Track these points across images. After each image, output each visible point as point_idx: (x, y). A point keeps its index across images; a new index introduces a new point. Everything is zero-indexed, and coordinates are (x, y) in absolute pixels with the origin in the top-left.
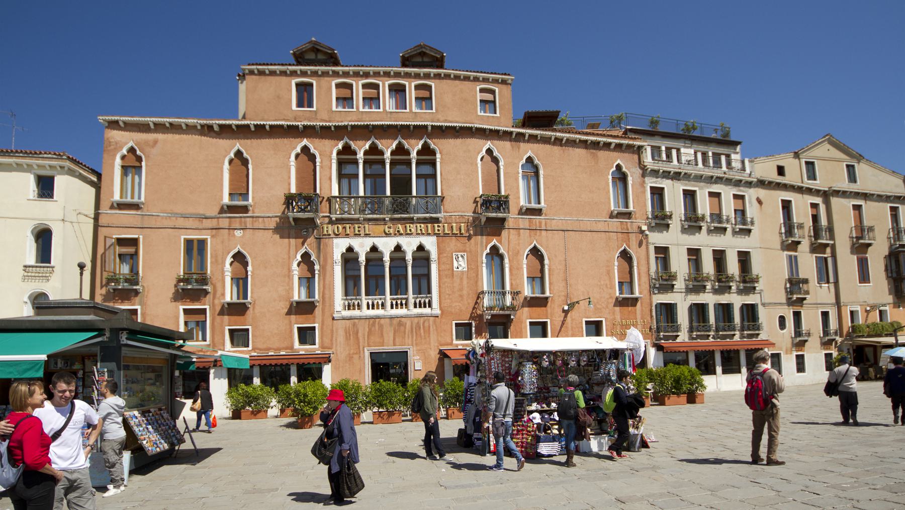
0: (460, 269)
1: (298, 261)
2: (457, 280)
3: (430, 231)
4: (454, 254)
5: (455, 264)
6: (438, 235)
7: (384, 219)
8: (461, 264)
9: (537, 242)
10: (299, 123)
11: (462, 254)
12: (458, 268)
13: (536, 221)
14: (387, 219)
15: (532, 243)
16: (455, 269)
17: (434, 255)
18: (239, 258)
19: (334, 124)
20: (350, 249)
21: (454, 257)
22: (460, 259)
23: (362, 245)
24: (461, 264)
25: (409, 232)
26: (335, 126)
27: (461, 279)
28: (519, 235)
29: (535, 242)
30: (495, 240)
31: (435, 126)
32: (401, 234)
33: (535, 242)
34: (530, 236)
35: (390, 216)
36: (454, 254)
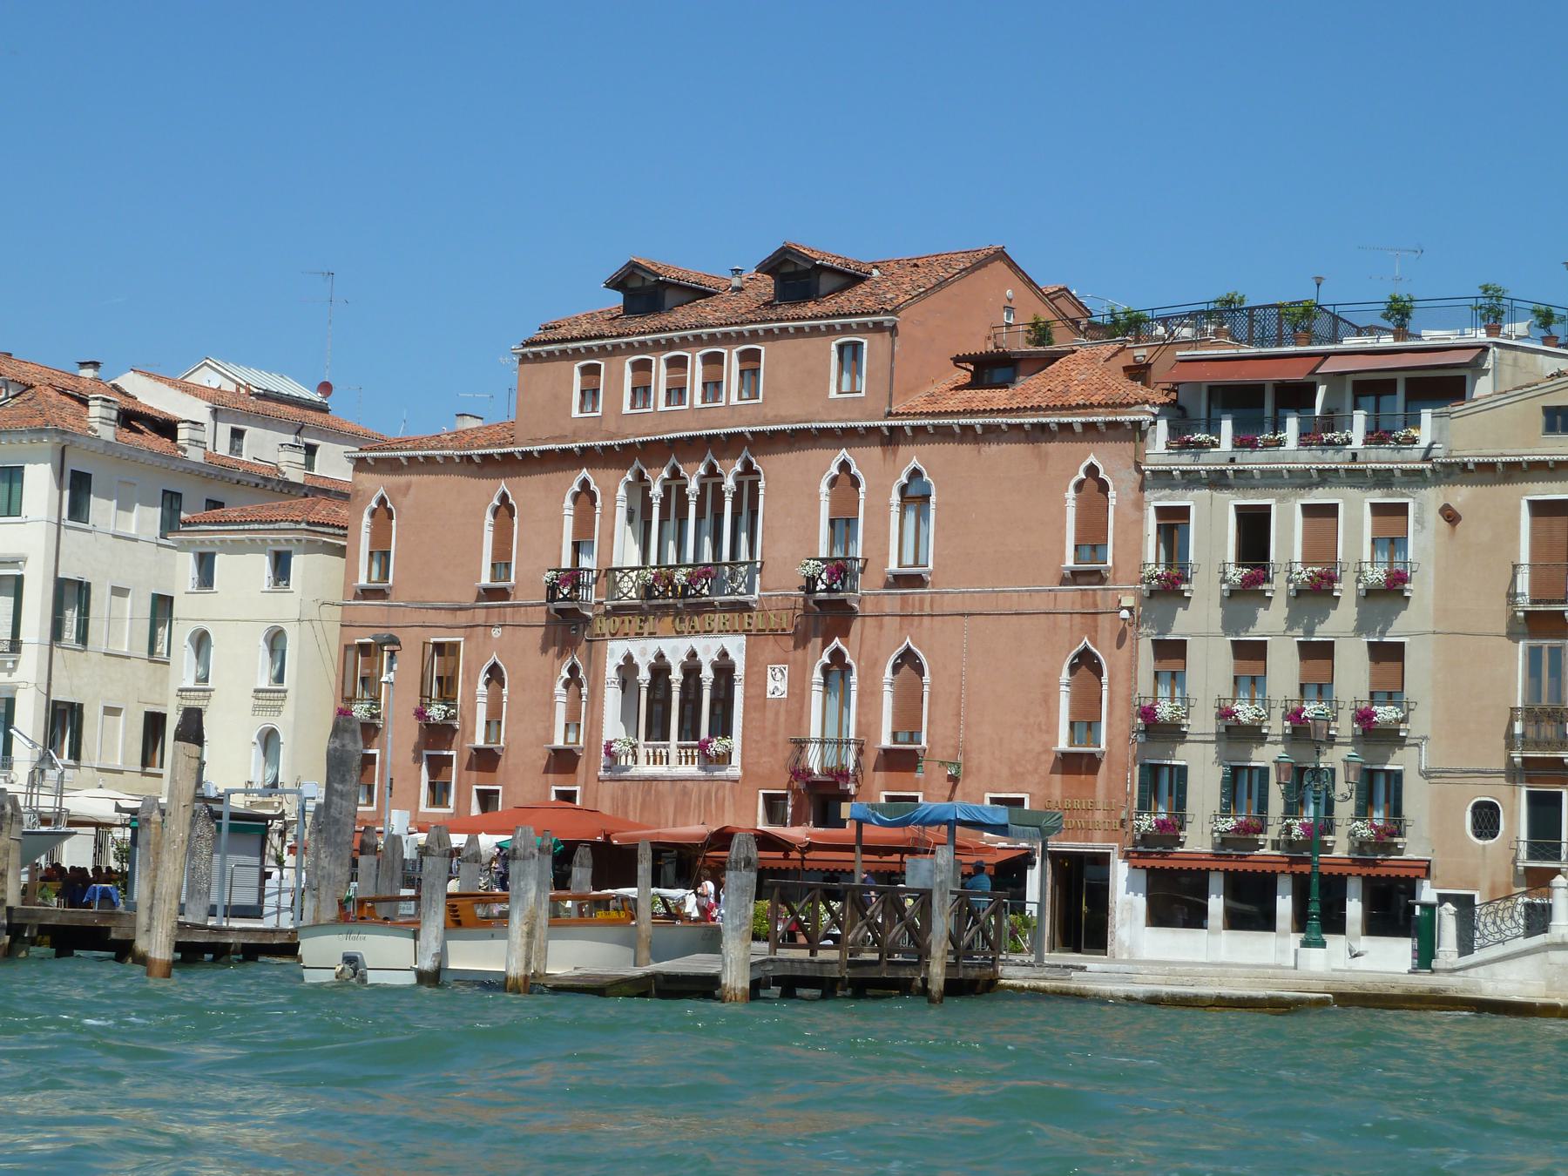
0: (777, 693)
2: (770, 715)
5: (770, 687)
8: (777, 684)
9: (911, 639)
11: (782, 666)
13: (913, 599)
16: (769, 696)
17: (740, 671)
20: (629, 658)
24: (777, 684)
27: (777, 714)
28: (881, 627)
29: (908, 640)
32: (697, 632)
33: (908, 640)
34: (901, 628)
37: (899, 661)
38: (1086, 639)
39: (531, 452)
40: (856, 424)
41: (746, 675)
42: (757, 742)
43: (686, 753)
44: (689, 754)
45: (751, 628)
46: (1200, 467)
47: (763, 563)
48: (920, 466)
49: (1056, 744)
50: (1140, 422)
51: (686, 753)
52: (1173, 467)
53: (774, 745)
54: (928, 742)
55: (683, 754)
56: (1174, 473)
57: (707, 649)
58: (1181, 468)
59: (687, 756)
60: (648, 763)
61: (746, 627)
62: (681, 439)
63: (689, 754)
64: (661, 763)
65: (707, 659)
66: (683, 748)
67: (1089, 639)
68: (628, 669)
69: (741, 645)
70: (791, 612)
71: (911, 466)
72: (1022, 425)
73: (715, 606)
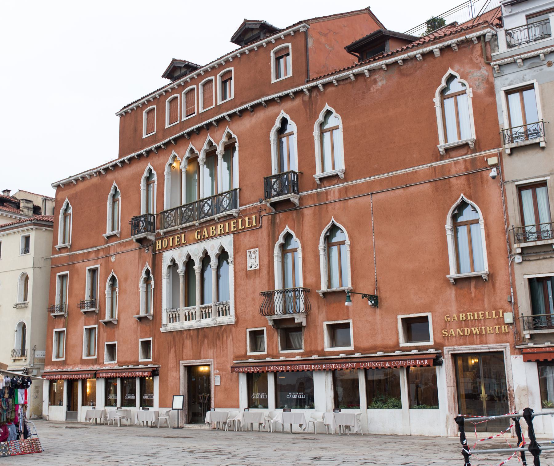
0: (253, 267)
1: (143, 278)
3: (227, 231)
4: (247, 251)
5: (250, 262)
6: (234, 233)
7: (195, 225)
10: (142, 151)
11: (255, 249)
12: (251, 267)
14: (197, 224)
15: (329, 221)
16: (249, 269)
18: (113, 279)
19: (162, 143)
20: (173, 261)
21: (248, 253)
22: (253, 256)
23: (180, 257)
25: (211, 235)
26: (164, 144)
29: (333, 219)
30: (287, 227)
31: (241, 110)
33: (333, 219)
35: (198, 221)
36: (247, 251)
37: (328, 234)
38: (462, 195)
39: (124, 160)
40: (288, 92)
41: (235, 259)
42: (244, 299)
43: (205, 311)
44: (207, 311)
45: (236, 229)
46: (539, 52)
47: (240, 189)
48: (330, 108)
49: (449, 274)
50: (484, 36)
51: (205, 311)
52: (516, 58)
53: (253, 299)
54: (352, 284)
55: (204, 312)
56: (518, 61)
57: (213, 246)
58: (523, 56)
59: (205, 313)
60: (186, 320)
61: (232, 229)
62: (193, 130)
63: (207, 311)
64: (193, 319)
65: (213, 254)
66: (203, 308)
67: (465, 194)
68: (174, 265)
69: (230, 241)
70: (258, 215)
71: (325, 110)
72: (396, 62)
73: (216, 220)
